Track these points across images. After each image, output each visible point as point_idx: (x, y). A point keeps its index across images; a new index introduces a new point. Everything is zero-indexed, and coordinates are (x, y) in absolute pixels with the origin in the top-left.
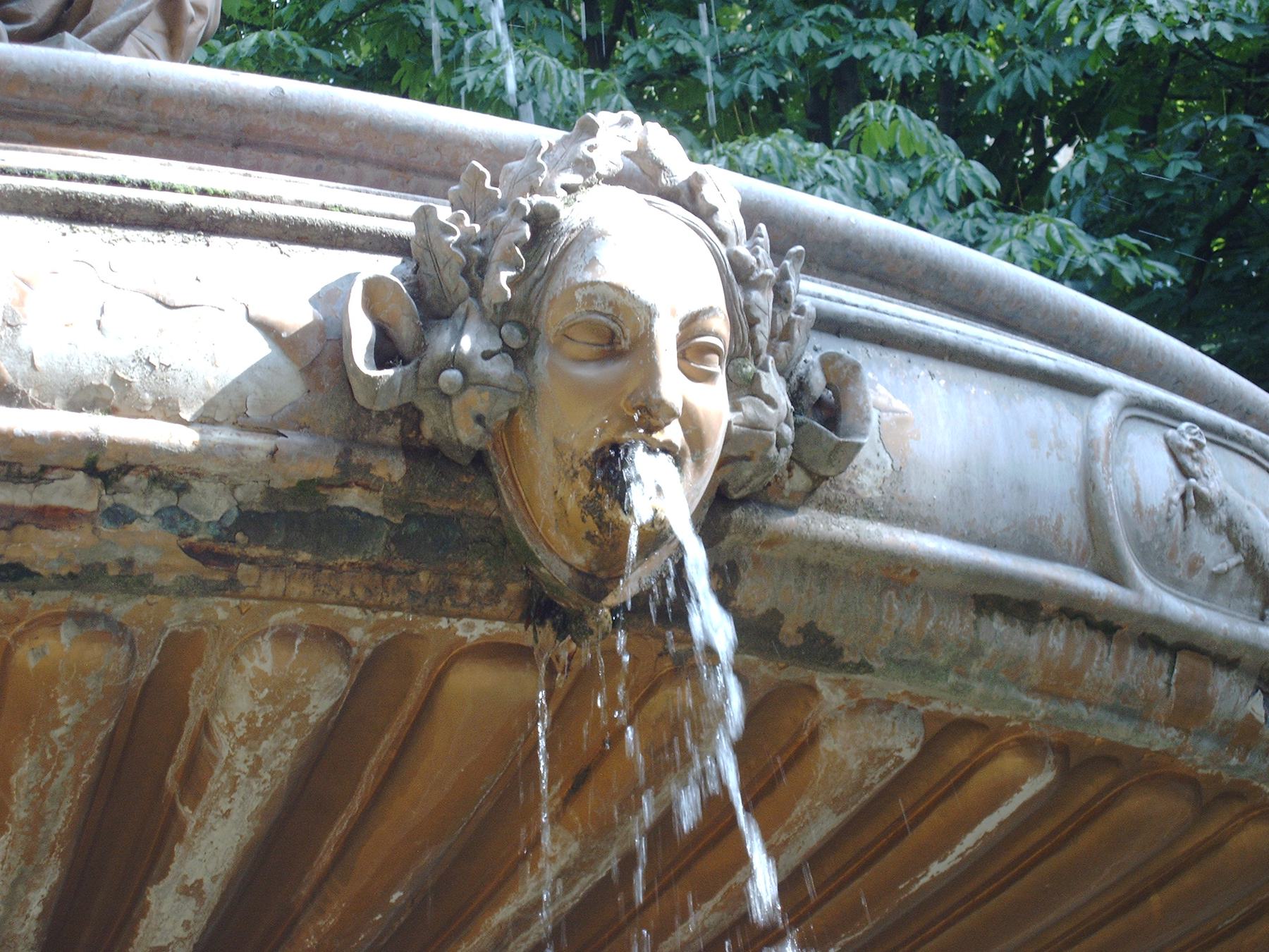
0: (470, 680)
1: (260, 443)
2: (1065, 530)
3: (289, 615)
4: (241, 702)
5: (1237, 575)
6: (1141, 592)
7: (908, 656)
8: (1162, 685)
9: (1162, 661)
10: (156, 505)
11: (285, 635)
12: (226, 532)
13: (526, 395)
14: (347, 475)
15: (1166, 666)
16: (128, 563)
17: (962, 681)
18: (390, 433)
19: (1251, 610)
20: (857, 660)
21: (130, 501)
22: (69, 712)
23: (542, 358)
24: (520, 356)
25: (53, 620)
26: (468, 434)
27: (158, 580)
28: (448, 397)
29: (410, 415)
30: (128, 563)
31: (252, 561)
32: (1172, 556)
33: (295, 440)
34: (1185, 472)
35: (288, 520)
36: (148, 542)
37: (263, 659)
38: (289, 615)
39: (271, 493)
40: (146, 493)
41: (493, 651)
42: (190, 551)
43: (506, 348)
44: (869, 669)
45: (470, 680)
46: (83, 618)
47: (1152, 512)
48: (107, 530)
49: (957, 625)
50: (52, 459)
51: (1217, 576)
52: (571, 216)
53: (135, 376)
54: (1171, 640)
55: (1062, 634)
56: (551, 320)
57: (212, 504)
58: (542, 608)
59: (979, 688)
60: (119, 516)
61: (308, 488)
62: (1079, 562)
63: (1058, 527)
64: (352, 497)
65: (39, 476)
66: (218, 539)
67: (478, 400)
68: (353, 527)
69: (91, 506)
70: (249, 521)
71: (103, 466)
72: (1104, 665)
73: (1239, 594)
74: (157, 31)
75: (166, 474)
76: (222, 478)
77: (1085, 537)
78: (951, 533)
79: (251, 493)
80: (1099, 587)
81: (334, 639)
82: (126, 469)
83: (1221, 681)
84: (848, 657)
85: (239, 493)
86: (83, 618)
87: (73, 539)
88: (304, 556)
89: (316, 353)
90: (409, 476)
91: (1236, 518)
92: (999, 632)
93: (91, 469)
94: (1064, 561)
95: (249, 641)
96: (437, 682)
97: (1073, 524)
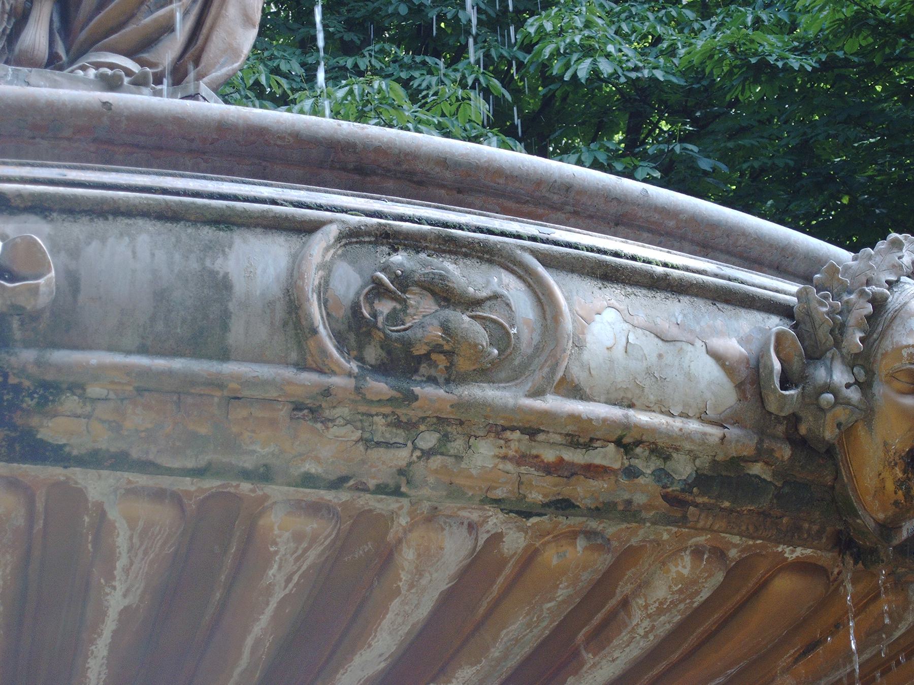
0: (784, 584)
1: (715, 432)
3: (701, 539)
4: (661, 591)
10: (653, 467)
11: (697, 552)
12: (688, 487)
13: (868, 413)
14: (761, 455)
16: (629, 502)
18: (780, 429)
21: (638, 463)
22: (562, 593)
23: (880, 389)
24: (865, 386)
25: (573, 535)
26: (829, 434)
27: (644, 514)
28: (821, 409)
29: (794, 420)
30: (629, 502)
31: (696, 505)
33: (733, 432)
35: (722, 479)
36: (644, 491)
37: (684, 566)
38: (701, 539)
39: (714, 463)
40: (648, 459)
41: (802, 567)
42: (665, 497)
43: (857, 382)
45: (784, 584)
46: (590, 534)
48: (623, 481)
50: (599, 434)
52: (895, 299)
53: (647, 383)
56: (883, 367)
57: (683, 469)
58: (846, 543)
60: (631, 473)
61: (736, 462)
64: (757, 469)
65: (588, 445)
66: (683, 490)
67: (841, 413)
68: (755, 486)
69: (617, 466)
70: (701, 480)
71: (626, 440)
75: (660, 448)
76: (690, 452)
79: (703, 462)
81: (719, 554)
82: (638, 443)
85: (698, 462)
86: (590, 534)
87: (600, 485)
88: (726, 504)
89: (749, 378)
90: (792, 458)
93: (619, 443)
95: (677, 553)
96: (763, 585)
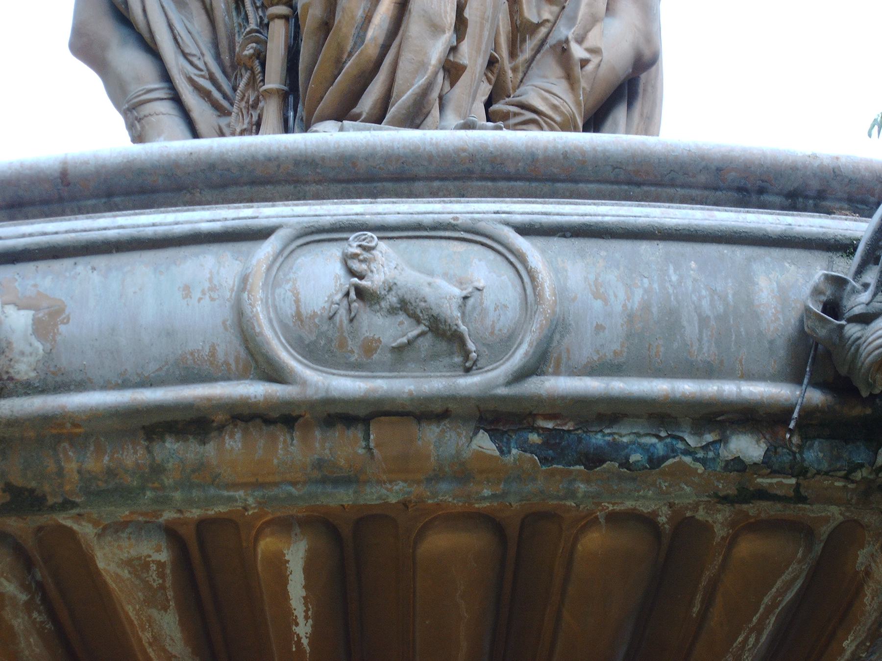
2: (221, 356)
5: (425, 343)
6: (304, 383)
7: (102, 486)
8: (361, 451)
9: (356, 433)
15: (360, 435)
17: (160, 493)
19: (453, 367)
20: (60, 500)
32: (342, 344)
34: (352, 273)
44: (74, 505)
47: (315, 315)
49: (132, 456)
51: (399, 350)
54: (362, 412)
55: (238, 436)
59: (177, 495)
62: (242, 375)
63: (213, 353)
72: (290, 451)
73: (435, 356)
74: (558, 78)
77: (243, 353)
78: (107, 386)
80: (255, 390)
83: (431, 433)
84: (51, 501)
91: (408, 297)
92: (173, 450)
94: (227, 378)
97: (228, 347)
